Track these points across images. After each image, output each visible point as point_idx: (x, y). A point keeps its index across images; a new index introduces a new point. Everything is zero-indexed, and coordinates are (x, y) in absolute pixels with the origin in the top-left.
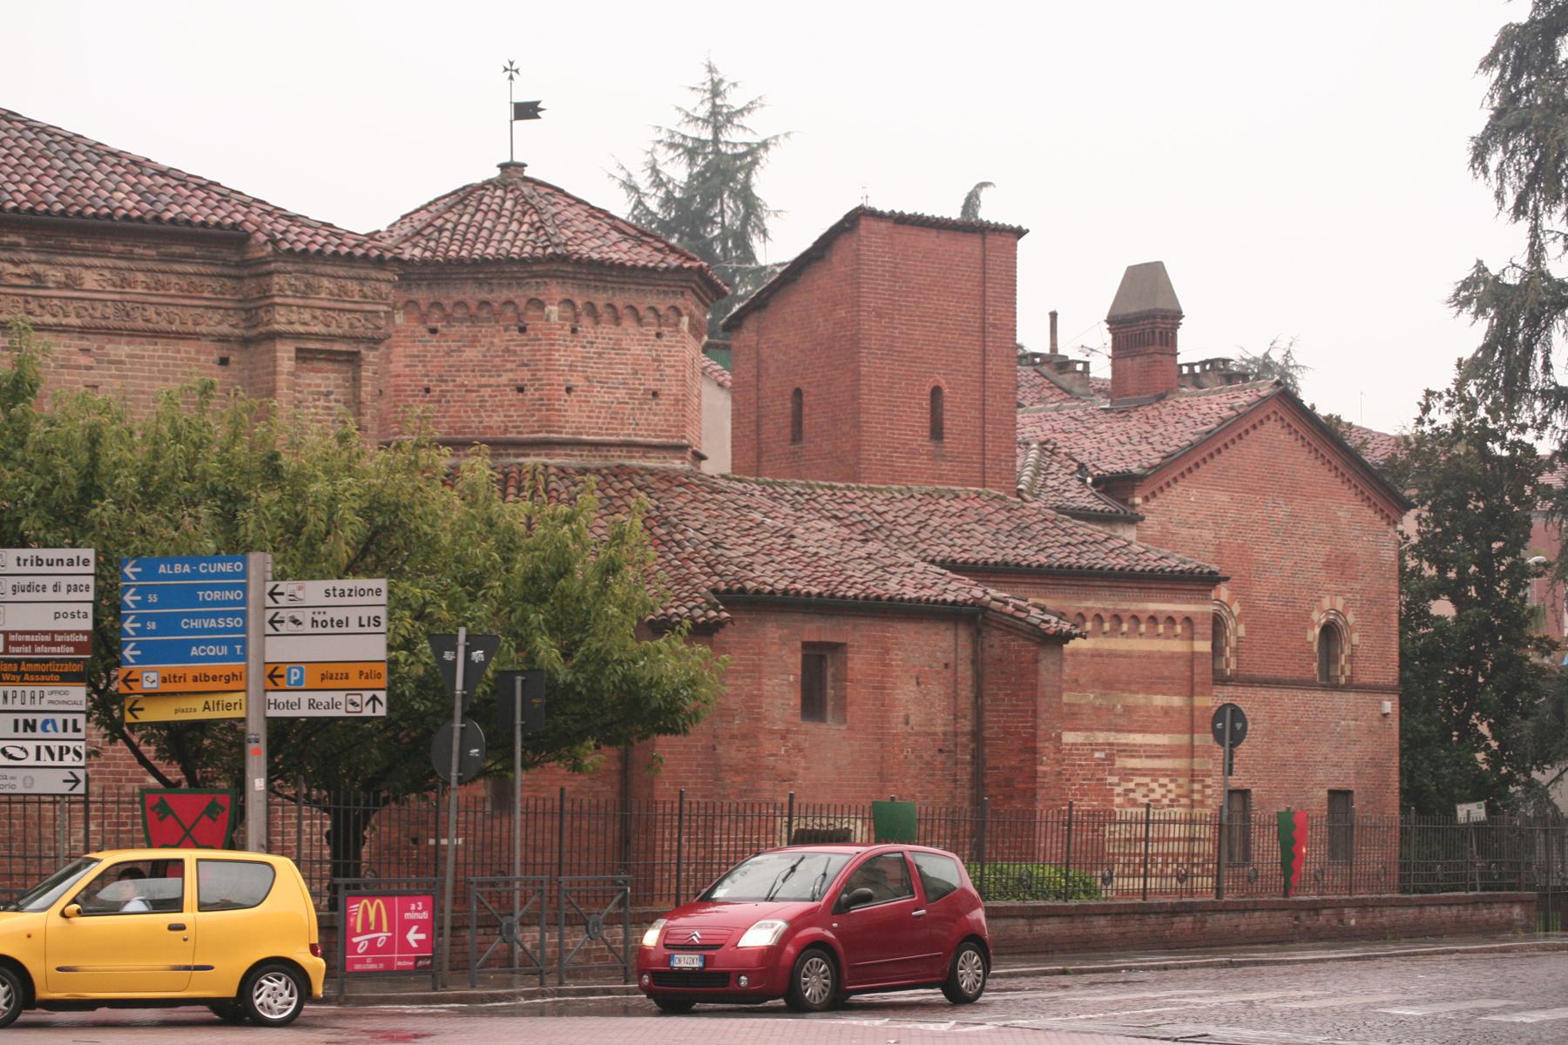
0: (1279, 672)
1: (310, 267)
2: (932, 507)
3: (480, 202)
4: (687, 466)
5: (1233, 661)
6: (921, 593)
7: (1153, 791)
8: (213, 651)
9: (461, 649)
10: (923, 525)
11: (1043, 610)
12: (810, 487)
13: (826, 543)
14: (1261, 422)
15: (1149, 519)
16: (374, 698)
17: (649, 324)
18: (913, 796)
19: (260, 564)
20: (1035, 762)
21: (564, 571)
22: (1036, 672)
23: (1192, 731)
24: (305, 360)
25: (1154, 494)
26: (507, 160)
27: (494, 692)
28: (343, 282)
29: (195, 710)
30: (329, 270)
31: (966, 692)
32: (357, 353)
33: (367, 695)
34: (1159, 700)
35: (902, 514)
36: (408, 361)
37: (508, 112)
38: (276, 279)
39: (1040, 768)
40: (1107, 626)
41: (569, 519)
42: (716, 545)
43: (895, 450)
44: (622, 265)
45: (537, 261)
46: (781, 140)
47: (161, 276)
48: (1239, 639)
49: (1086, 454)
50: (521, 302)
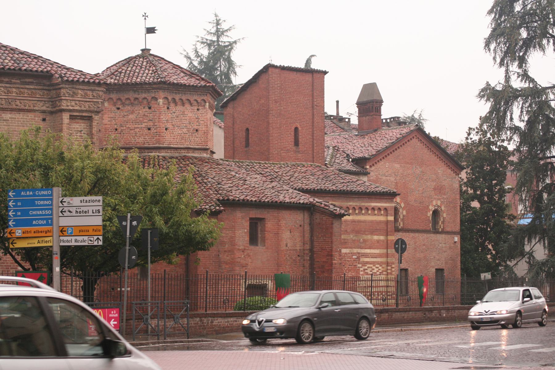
1: (74, 86)
2: (295, 170)
3: (134, 63)
4: (208, 156)
5: (401, 223)
6: (291, 200)
7: (374, 269)
8: (41, 222)
9: (129, 221)
10: (292, 176)
11: (335, 206)
12: (252, 163)
13: (258, 183)
14: (411, 139)
15: (372, 174)
16: (98, 239)
17: (194, 106)
18: (289, 272)
19: (57, 191)
20: (332, 260)
21: (165, 193)
22: (332, 228)
23: (387, 248)
24: (73, 119)
25: (373, 165)
26: (144, 48)
27: (140, 236)
28: (86, 91)
29: (34, 243)
30: (81, 87)
31: (307, 235)
32: (91, 117)
33: (96, 237)
34: (376, 237)
35: (284, 172)
36: (109, 119)
37: (144, 31)
38: (62, 90)
39: (334, 262)
40: (357, 212)
41: (166, 175)
42: (219, 184)
43: (282, 150)
44: (185, 85)
45: (155, 83)
46: (241, 40)
47: (21, 90)
48: (404, 216)
49: (349, 151)
50: (149, 98)
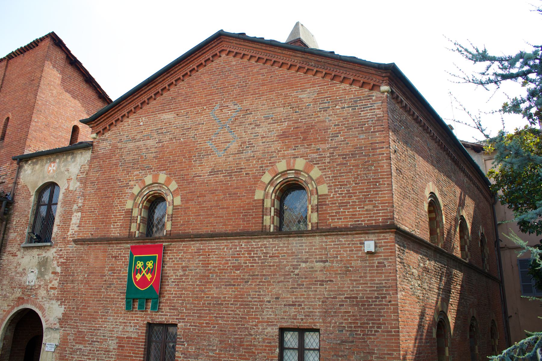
0: (220, 228)
48: (175, 208)
